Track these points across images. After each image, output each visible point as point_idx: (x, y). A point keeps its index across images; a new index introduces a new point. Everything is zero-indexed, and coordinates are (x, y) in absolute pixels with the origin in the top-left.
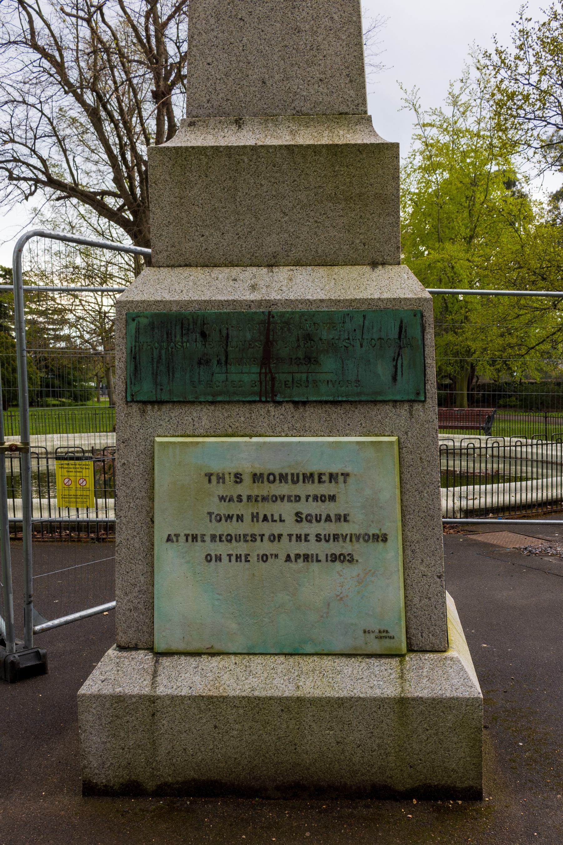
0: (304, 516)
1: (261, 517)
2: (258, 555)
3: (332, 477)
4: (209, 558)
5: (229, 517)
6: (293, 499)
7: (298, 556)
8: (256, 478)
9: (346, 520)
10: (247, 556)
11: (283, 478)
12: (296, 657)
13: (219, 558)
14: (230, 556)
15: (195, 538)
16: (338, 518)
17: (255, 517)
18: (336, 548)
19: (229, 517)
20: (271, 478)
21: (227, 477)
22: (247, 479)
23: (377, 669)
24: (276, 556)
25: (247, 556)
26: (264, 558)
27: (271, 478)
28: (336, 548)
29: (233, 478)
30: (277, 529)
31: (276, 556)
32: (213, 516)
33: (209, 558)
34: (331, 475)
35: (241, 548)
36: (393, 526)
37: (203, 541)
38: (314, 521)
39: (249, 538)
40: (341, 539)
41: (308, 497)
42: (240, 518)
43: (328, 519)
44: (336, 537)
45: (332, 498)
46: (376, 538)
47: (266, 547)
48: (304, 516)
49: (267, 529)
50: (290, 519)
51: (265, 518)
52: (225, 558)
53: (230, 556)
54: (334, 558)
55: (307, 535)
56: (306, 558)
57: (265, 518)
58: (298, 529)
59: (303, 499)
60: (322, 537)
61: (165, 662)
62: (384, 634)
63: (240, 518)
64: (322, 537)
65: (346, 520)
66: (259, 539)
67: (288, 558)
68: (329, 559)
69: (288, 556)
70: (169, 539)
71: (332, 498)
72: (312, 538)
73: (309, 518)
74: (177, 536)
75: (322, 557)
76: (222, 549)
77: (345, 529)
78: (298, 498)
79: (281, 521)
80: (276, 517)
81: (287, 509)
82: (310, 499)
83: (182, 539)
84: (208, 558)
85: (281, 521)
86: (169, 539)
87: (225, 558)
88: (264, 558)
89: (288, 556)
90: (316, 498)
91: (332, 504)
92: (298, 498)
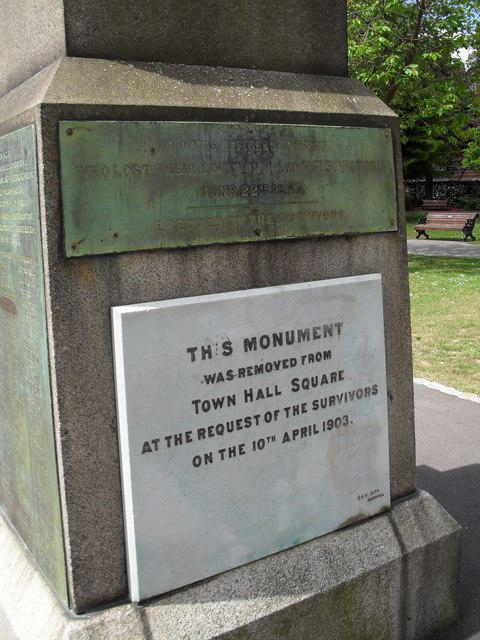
0: (300, 383)
2: (254, 443)
3: (328, 331)
4: (197, 462)
5: (218, 403)
7: (295, 433)
8: (249, 344)
9: (341, 379)
11: (278, 339)
12: (297, 549)
13: (209, 458)
15: (178, 440)
16: (333, 377)
18: (330, 413)
19: (218, 403)
20: (265, 342)
21: (213, 349)
22: (238, 346)
24: (274, 438)
25: (241, 446)
26: (259, 445)
27: (265, 341)
28: (330, 413)
30: (271, 404)
31: (274, 438)
32: (200, 405)
33: (197, 462)
38: (310, 386)
39: (243, 424)
40: (336, 401)
41: (304, 357)
42: (232, 400)
43: (325, 381)
45: (327, 355)
48: (300, 383)
49: (271, 404)
51: (260, 395)
52: (216, 457)
54: (331, 424)
56: (304, 431)
57: (260, 395)
60: (319, 403)
63: (232, 400)
64: (319, 403)
65: (341, 379)
66: (253, 421)
67: (286, 438)
68: (326, 427)
70: (146, 449)
71: (327, 355)
73: (306, 383)
74: (155, 442)
75: (319, 428)
76: (212, 445)
79: (278, 393)
80: (272, 391)
81: (282, 378)
82: (307, 360)
83: (163, 443)
84: (196, 462)
85: (278, 393)
87: (216, 457)
88: (259, 445)
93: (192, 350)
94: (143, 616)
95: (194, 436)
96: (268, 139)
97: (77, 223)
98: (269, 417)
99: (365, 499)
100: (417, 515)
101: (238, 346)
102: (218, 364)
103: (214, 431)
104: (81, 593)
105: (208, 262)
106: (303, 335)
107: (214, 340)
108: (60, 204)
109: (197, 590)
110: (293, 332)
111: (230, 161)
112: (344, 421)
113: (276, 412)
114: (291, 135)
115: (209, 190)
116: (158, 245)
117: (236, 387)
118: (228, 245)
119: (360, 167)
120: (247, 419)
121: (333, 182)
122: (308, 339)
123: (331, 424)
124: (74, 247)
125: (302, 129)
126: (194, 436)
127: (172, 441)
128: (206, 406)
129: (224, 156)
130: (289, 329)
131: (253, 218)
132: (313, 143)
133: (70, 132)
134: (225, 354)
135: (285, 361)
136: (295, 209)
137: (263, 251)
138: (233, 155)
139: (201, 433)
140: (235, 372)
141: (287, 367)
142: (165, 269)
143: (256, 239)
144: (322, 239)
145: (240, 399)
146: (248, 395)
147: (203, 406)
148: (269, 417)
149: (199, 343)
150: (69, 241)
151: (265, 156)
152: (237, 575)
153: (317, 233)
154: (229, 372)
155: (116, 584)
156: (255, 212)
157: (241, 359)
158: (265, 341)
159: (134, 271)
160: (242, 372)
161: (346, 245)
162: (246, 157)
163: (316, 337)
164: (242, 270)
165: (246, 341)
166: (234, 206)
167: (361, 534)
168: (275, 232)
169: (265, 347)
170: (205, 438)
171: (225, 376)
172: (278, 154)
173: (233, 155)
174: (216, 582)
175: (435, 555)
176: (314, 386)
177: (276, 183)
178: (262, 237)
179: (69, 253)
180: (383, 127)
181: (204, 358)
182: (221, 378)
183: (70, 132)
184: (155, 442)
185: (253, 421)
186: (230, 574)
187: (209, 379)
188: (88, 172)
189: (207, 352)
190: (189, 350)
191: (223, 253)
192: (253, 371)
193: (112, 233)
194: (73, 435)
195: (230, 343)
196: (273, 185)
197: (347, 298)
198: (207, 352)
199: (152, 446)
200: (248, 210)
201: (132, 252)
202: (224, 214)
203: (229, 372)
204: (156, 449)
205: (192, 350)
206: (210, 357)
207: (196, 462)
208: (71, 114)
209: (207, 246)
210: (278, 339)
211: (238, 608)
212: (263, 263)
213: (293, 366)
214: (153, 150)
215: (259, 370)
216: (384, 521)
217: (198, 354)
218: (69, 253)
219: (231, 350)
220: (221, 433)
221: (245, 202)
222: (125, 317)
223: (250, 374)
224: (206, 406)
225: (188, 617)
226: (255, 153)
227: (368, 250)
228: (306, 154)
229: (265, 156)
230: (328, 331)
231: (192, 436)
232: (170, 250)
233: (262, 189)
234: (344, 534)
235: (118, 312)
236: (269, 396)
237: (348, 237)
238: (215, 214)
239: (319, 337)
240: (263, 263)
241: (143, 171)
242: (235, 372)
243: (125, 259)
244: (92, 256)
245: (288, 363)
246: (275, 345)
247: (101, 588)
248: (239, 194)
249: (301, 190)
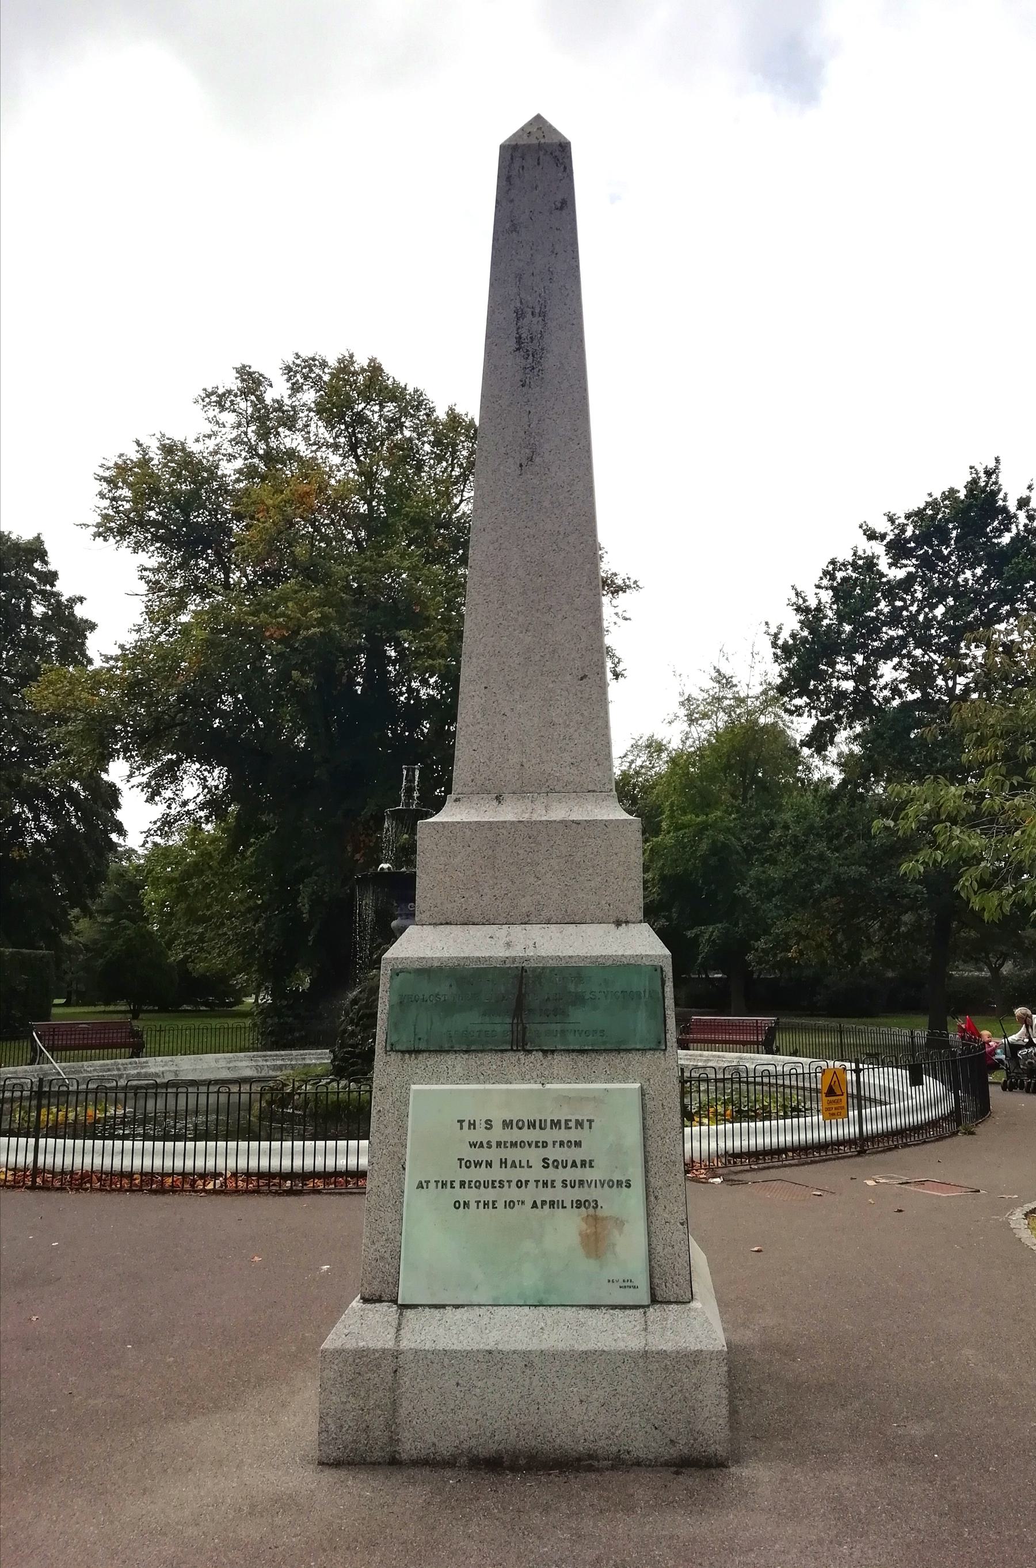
0: (550, 1162)
1: (570, 1164)
5: (478, 1164)
6: (540, 1144)
7: (544, 1203)
8: (507, 1124)
9: (591, 1166)
10: (494, 1202)
11: (532, 1125)
13: (466, 1204)
14: (478, 1202)
15: (444, 1185)
16: (583, 1164)
17: (503, 1163)
19: (478, 1164)
21: (477, 1123)
22: (497, 1125)
23: (621, 1320)
24: (523, 1203)
25: (494, 1202)
26: (510, 1204)
29: (484, 1125)
30: (523, 1174)
31: (523, 1203)
32: (463, 1162)
34: (577, 1121)
35: (489, 1194)
36: (636, 1174)
37: (452, 1187)
38: (560, 1166)
39: (497, 1184)
41: (554, 1143)
42: (489, 1164)
43: (574, 1164)
44: (581, 1183)
45: (578, 1144)
46: (619, 1183)
47: (513, 1193)
48: (550, 1162)
49: (516, 1174)
50: (537, 1164)
52: (473, 1205)
53: (478, 1202)
54: (579, 1204)
55: (553, 1181)
56: (552, 1204)
58: (550, 1174)
59: (550, 1144)
61: (409, 1314)
62: (629, 1284)
63: (489, 1164)
64: (568, 1183)
65: (591, 1166)
66: (506, 1184)
67: (535, 1205)
69: (535, 1202)
70: (420, 1186)
71: (578, 1144)
72: (558, 1184)
74: (428, 1182)
75: (568, 1204)
76: (469, 1195)
77: (588, 1174)
78: (545, 1144)
80: (524, 1163)
81: (534, 1155)
83: (432, 1185)
84: (457, 1205)
86: (420, 1186)
87: (473, 1205)
88: (510, 1204)
89: (535, 1202)
90: (562, 1144)
91: (578, 1149)
92: (545, 1144)
93: (461, 1122)
95: (457, 1185)
98: (519, 1184)
99: (617, 1285)
101: (497, 1125)
102: (480, 1135)
103: (473, 1185)
106: (555, 1124)
110: (545, 1121)
113: (527, 1182)
117: (494, 1155)
120: (500, 1182)
123: (579, 1204)
126: (457, 1185)
135: (537, 1142)
139: (462, 1184)
145: (496, 1164)
146: (503, 1163)
148: (519, 1184)
149: (468, 1117)
154: (489, 1143)
157: (498, 1133)
160: (499, 1144)
163: (568, 1128)
167: (607, 1316)
169: (520, 1129)
171: (485, 1145)
182: (481, 1145)
184: (428, 1182)
185: (506, 1184)
187: (473, 1145)
198: (472, 1125)
199: (425, 1185)
203: (489, 1143)
205: (461, 1122)
210: (532, 1125)
215: (514, 1144)
217: (466, 1125)
219: (491, 1126)
222: (416, 1091)
228: (572, 987)
235: (413, 1087)
245: (540, 1144)
247: (376, 1288)
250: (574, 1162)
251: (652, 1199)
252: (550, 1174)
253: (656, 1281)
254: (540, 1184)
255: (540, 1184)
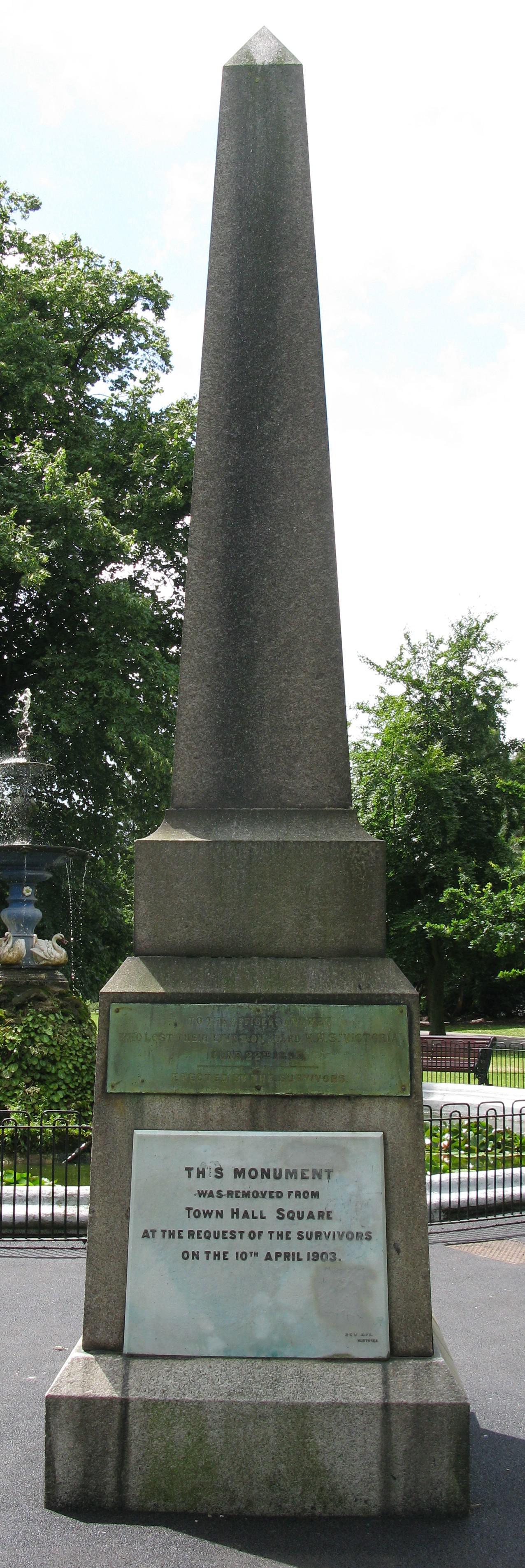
0: (285, 1213)
1: (241, 1214)
2: (237, 1253)
4: (186, 1255)
5: (208, 1214)
6: (274, 1195)
7: (278, 1255)
9: (329, 1218)
10: (225, 1253)
11: (266, 1173)
12: (274, 1361)
13: (196, 1255)
14: (208, 1253)
15: (172, 1234)
16: (321, 1215)
17: (235, 1213)
18: (319, 1246)
19: (208, 1214)
20: (253, 1174)
21: (207, 1171)
22: (228, 1174)
23: (359, 1374)
24: (256, 1254)
25: (225, 1253)
26: (243, 1256)
27: (253, 1173)
28: (319, 1246)
29: (213, 1173)
31: (256, 1254)
32: (192, 1212)
33: (186, 1255)
34: (314, 1171)
35: (219, 1246)
36: (377, 1224)
37: (180, 1237)
38: (296, 1218)
39: (228, 1235)
41: (290, 1193)
42: (220, 1214)
43: (311, 1216)
44: (318, 1235)
45: (315, 1195)
46: (359, 1235)
47: (245, 1244)
48: (285, 1213)
49: (247, 1225)
50: (271, 1215)
51: (246, 1215)
52: (202, 1256)
53: (208, 1253)
54: (316, 1256)
55: (288, 1233)
56: (287, 1256)
57: (246, 1215)
59: (285, 1194)
60: (304, 1235)
62: (368, 1338)
63: (220, 1214)
64: (304, 1235)
65: (329, 1218)
66: (238, 1235)
67: (268, 1257)
68: (311, 1257)
69: (269, 1254)
70: (146, 1235)
71: (315, 1195)
72: (294, 1235)
73: (291, 1215)
74: (153, 1231)
75: (304, 1256)
76: (199, 1246)
77: (325, 1226)
78: (280, 1195)
79: (262, 1217)
80: (257, 1214)
81: (269, 1206)
82: (293, 1195)
83: (159, 1234)
84: (185, 1255)
85: (262, 1217)
86: (146, 1235)
87: (202, 1256)
88: (243, 1256)
89: (269, 1254)
90: (298, 1194)
91: (315, 1200)
92: (280, 1195)
93: (189, 1170)
94: (127, 1366)
95: (185, 1234)
96: (273, 1017)
97: (116, 1070)
98: (252, 1235)
99: (354, 1339)
100: (417, 1374)
101: (228, 1174)
102: (209, 1183)
103: (202, 1235)
104: (88, 1334)
105: (214, 1108)
106: (291, 1174)
107: (209, 1165)
108: (106, 1057)
109: (175, 1362)
111: (238, 1033)
112: (330, 1257)
113: (260, 1233)
114: (296, 1013)
115: (217, 1054)
116: (173, 1090)
117: (226, 1205)
118: (232, 1096)
119: (368, 1040)
120: (232, 1232)
121: (335, 1051)
122: (296, 1178)
123: (316, 1256)
124: (113, 1087)
125: (306, 1009)
127: (167, 1234)
128: (197, 1214)
129: (233, 1029)
130: (278, 1167)
131: (255, 1077)
132: (317, 1018)
133: (117, 1011)
134: (217, 1177)
135: (271, 1192)
136: (295, 1071)
137: (263, 1104)
138: (241, 1028)
139: (191, 1234)
140: (225, 1193)
141: (273, 1197)
142: (180, 1108)
143: (257, 1093)
144: (319, 1097)
145: (227, 1214)
146: (235, 1213)
147: (194, 1213)
148: (252, 1235)
149: (195, 1165)
150: (109, 1082)
151: (269, 1029)
152: (213, 1363)
153: (315, 1093)
154: (219, 1192)
155: (116, 1337)
156: (257, 1072)
157: (229, 1183)
158: (253, 1173)
159: (155, 1107)
160: (230, 1194)
161: (349, 1105)
162: (252, 1030)
163: (303, 1177)
164: (244, 1115)
165: (236, 1171)
166: (238, 1067)
167: (345, 1370)
168: (275, 1089)
169: (253, 1178)
170: (199, 1237)
171: (215, 1194)
172: (282, 1028)
173: (241, 1028)
174: (192, 1361)
175: (428, 1419)
176: (299, 1218)
177: (278, 1051)
178: (262, 1092)
179: (109, 1090)
180: (399, 1004)
181: (198, 1177)
182: (211, 1195)
183: (117, 1011)
184: (153, 1231)
185: (238, 1235)
186: (207, 1360)
187: (201, 1194)
188: (126, 1037)
189: (201, 1173)
190: (187, 1169)
191: (227, 1101)
192: (240, 1195)
193: (141, 1079)
194: (97, 1215)
195: (221, 1169)
196: (275, 1053)
197: (341, 1150)
198: (201, 1173)
199: (151, 1234)
200: (250, 1071)
201: (154, 1094)
202: (229, 1072)
203: (219, 1192)
204: (153, 1237)
205: (189, 1170)
206: (204, 1177)
207: (185, 1255)
208: (120, 999)
209: (213, 1095)
210: (266, 1173)
211: (203, 1387)
212: (263, 1113)
213: (278, 1197)
214: (176, 1025)
215: (246, 1195)
216: (377, 1368)
217: (194, 1173)
218: (109, 1090)
219: (222, 1175)
220: (208, 1238)
221: (248, 1064)
222: (141, 1137)
223: (237, 1197)
224: (197, 1214)
225: (160, 1378)
226: (261, 1027)
227: (376, 1111)
228: (309, 1029)
229: (269, 1029)
230: (317, 1174)
231: (183, 1234)
232: (182, 1095)
233: (264, 1055)
234: (327, 1365)
235: (137, 1132)
236: (254, 1217)
237: (348, 1097)
238: (221, 1072)
239: (307, 1178)
240: (263, 1113)
241: (167, 1038)
242: (225, 1193)
243: (148, 1098)
244: (124, 1094)
245: (274, 1195)
246: (262, 1177)
247: (103, 1336)
248: (244, 1058)
249: (302, 1057)
250: (311, 1213)
251: (394, 1251)
252: (284, 1226)
253: (396, 1335)
254: (275, 1235)
255: (275, 1235)
